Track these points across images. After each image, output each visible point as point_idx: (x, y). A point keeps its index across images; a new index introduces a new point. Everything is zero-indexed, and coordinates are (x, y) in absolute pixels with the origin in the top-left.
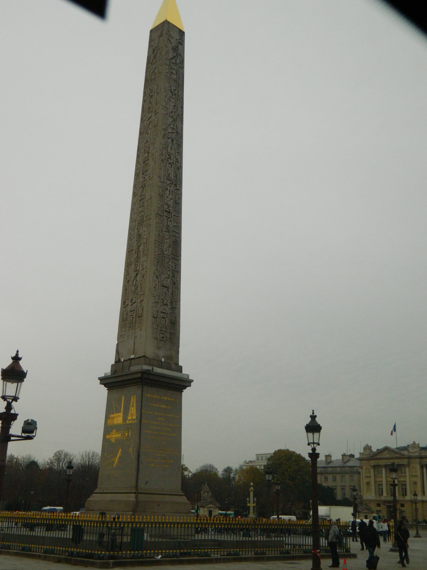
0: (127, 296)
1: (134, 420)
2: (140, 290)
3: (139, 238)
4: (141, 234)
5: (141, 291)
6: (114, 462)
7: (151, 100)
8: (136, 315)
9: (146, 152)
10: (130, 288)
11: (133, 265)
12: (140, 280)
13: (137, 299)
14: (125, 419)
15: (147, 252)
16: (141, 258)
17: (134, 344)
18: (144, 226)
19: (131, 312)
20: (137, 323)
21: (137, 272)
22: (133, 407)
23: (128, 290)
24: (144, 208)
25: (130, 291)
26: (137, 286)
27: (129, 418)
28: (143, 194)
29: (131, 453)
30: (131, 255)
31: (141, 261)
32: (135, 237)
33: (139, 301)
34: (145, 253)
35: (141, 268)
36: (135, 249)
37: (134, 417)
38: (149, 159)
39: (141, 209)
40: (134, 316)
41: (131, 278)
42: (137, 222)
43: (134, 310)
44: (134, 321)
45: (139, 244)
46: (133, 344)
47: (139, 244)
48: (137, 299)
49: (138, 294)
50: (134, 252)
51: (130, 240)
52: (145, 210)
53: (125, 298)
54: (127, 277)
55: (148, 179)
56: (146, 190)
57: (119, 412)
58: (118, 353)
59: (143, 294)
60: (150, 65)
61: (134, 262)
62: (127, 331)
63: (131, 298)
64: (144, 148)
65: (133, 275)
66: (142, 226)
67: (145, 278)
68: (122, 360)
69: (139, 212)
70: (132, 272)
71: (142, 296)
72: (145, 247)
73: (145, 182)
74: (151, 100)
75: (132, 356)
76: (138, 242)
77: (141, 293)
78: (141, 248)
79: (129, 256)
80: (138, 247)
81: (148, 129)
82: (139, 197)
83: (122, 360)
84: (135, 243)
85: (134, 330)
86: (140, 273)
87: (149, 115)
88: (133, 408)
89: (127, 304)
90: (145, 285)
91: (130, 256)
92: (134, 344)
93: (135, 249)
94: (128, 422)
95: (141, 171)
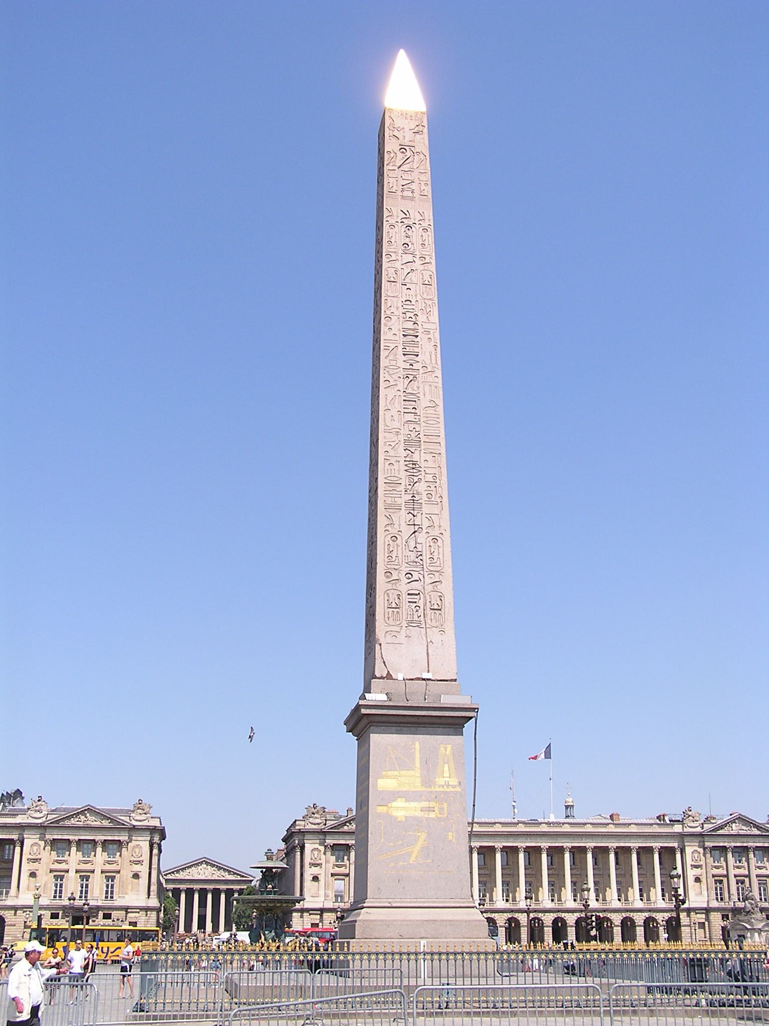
0: (393, 563)
1: (454, 787)
2: (429, 561)
3: (413, 469)
4: (418, 463)
5: (431, 565)
6: (409, 854)
7: (410, 233)
8: (425, 604)
9: (408, 319)
10: (400, 552)
11: (403, 512)
12: (428, 545)
13: (424, 577)
14: (427, 781)
15: (439, 500)
16: (423, 504)
17: (428, 653)
18: (423, 451)
19: (408, 594)
20: (429, 617)
21: (417, 527)
22: (444, 763)
23: (394, 554)
24: (416, 417)
25: (400, 557)
26: (420, 553)
27: (440, 781)
28: (410, 391)
29: (454, 841)
30: (395, 492)
31: (426, 509)
32: (402, 463)
33: (428, 580)
34: (433, 499)
35: (426, 523)
36: (403, 484)
37: (454, 781)
38: (417, 336)
39: (411, 417)
40: (421, 604)
41: (400, 533)
42: (401, 438)
43: (419, 594)
44: (421, 612)
45: (416, 479)
46: (426, 655)
47: (416, 479)
48: (424, 577)
49: (425, 567)
50: (402, 488)
51: (387, 463)
52: (423, 424)
53: (388, 566)
54: (389, 528)
55: (421, 371)
56: (418, 388)
57: (411, 768)
58: (384, 662)
59: (438, 571)
60: (396, 168)
61: (403, 508)
62: (404, 628)
63: (405, 569)
64: (401, 310)
65: (407, 531)
66: (420, 449)
67: (440, 543)
68: (400, 677)
69: (404, 420)
70: (403, 525)
71: (437, 574)
72: (433, 488)
73: (415, 373)
74: (410, 233)
75: (426, 675)
76: (412, 474)
77: (431, 568)
78: (421, 487)
79: (387, 492)
80: (412, 484)
81: (407, 280)
82: (401, 393)
83: (400, 677)
84: (403, 474)
85: (423, 631)
86: (425, 531)
87: (410, 258)
88: (446, 765)
89: (395, 577)
90: (441, 556)
91: (391, 492)
92: (428, 653)
93: (406, 486)
94: (437, 789)
95: (400, 347)
